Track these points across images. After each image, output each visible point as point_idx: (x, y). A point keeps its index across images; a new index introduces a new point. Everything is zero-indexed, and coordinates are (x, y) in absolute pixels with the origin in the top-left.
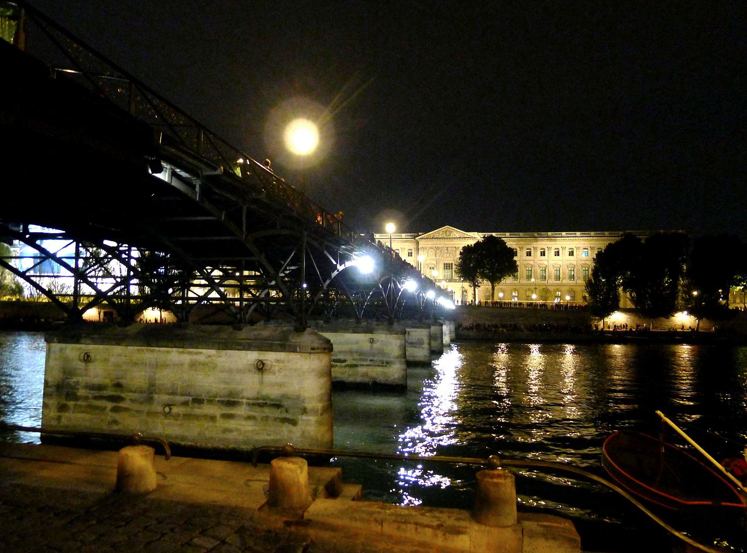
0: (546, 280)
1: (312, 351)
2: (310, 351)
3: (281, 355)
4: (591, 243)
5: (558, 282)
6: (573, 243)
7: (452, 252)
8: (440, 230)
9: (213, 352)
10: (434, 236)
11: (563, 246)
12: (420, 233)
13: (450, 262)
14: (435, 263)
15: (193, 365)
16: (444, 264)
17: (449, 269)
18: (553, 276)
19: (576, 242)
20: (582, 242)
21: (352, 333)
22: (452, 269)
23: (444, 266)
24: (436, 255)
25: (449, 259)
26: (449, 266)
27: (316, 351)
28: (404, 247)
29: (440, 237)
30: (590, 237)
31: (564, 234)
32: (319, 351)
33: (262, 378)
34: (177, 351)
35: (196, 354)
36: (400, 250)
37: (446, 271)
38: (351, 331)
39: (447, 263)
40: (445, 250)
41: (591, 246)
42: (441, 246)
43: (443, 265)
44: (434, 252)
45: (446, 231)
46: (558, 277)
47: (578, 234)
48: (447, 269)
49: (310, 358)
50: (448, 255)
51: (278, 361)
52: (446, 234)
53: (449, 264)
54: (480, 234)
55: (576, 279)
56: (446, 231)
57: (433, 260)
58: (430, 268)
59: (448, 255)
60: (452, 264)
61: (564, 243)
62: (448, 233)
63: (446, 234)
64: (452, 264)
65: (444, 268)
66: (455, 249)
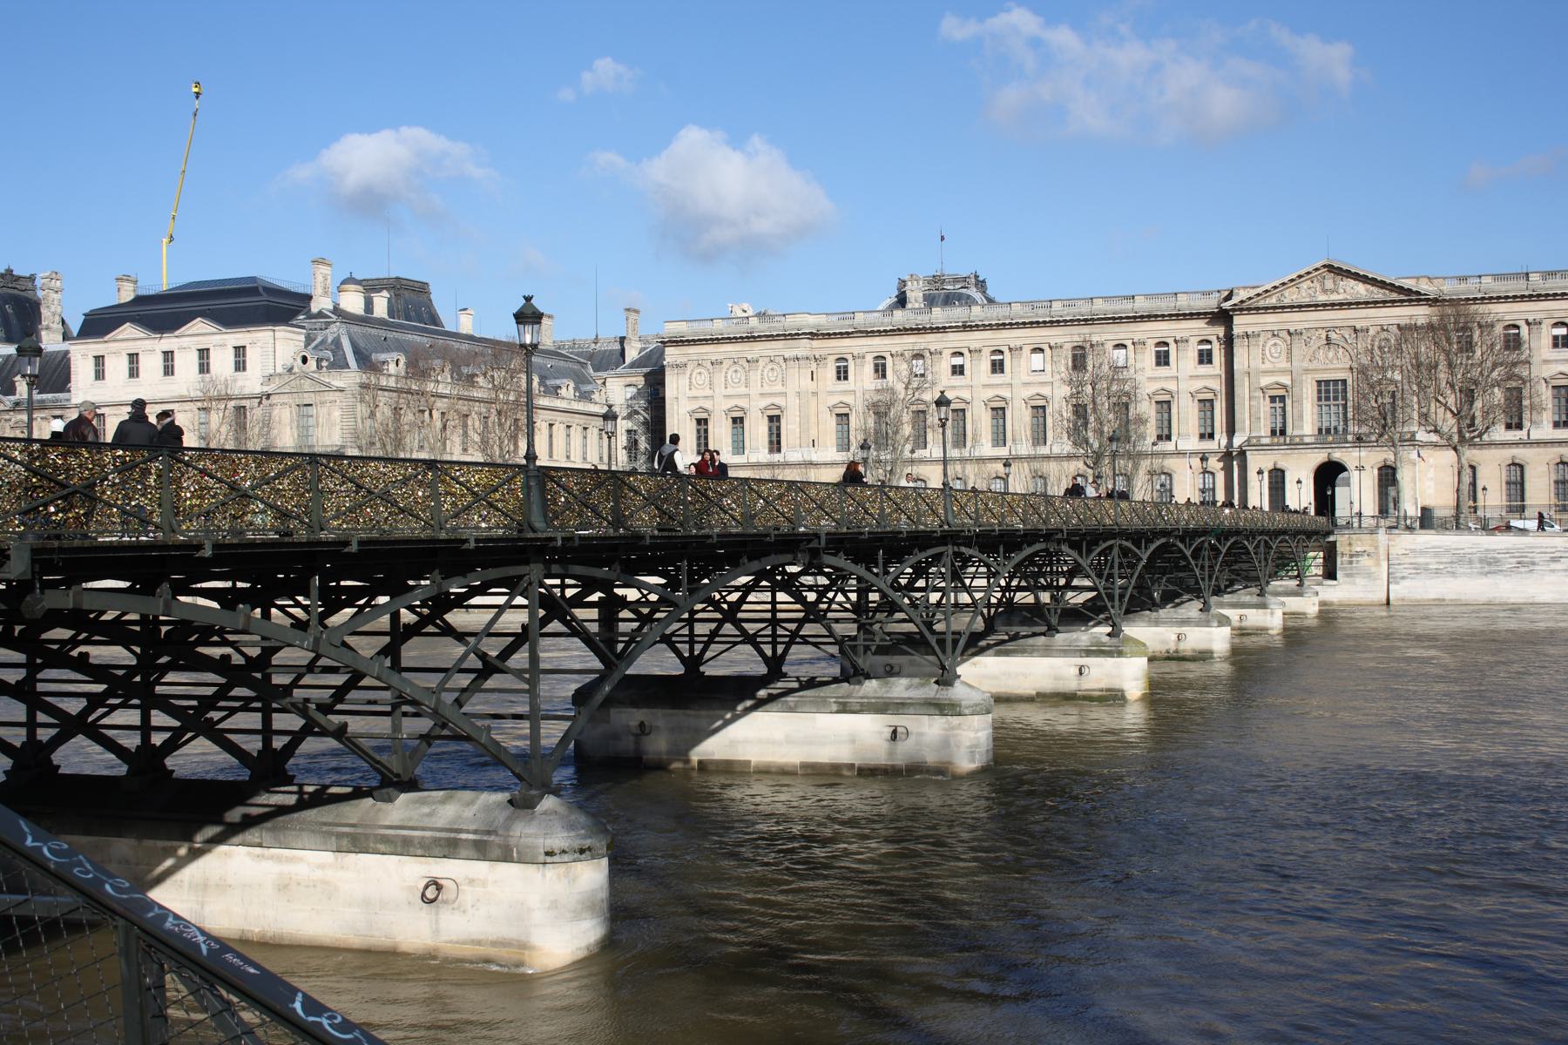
1: (549, 859)
2: (542, 858)
3: (480, 868)
9: (327, 857)
15: (283, 887)
21: (838, 712)
22: (1345, 398)
23: (1319, 392)
24: (1290, 358)
27: (556, 859)
32: (566, 858)
33: (437, 921)
34: (249, 854)
35: (290, 860)
38: (835, 707)
44: (1284, 346)
48: (1328, 399)
49: (544, 875)
50: (1331, 354)
51: (471, 882)
57: (1282, 372)
58: (1273, 399)
59: (1331, 354)
60: (1344, 381)
65: (1319, 399)
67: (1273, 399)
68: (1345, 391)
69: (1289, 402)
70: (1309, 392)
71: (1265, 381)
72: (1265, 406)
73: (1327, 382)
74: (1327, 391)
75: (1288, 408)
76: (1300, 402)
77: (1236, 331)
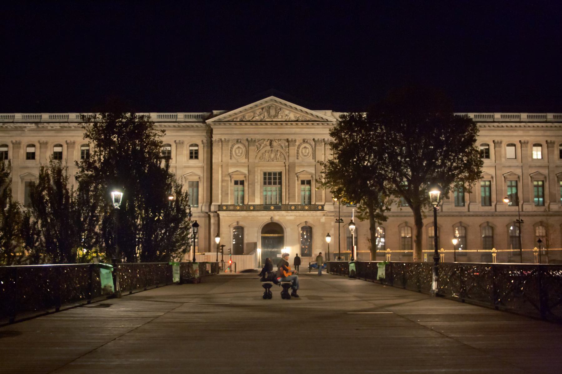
0: (466, 204)
4: (548, 133)
5: (487, 208)
6: (515, 134)
7: (280, 149)
8: (256, 106)
10: (244, 117)
11: (497, 139)
12: (215, 112)
13: (277, 170)
14: (246, 172)
16: (265, 174)
17: (275, 183)
18: (479, 199)
19: (520, 133)
20: (531, 133)
22: (280, 183)
23: (265, 179)
25: (275, 163)
26: (275, 179)
28: (181, 139)
29: (257, 118)
30: (494, 122)
31: (498, 116)
36: (38, 145)
37: (269, 188)
39: (269, 171)
40: (266, 145)
41: (549, 139)
42: (258, 137)
43: (263, 176)
44: (244, 149)
45: (269, 108)
46: (487, 199)
47: (524, 116)
48: (270, 183)
50: (272, 156)
52: (269, 112)
53: (275, 174)
54: (338, 114)
55: (521, 203)
56: (269, 108)
57: (242, 165)
58: (236, 183)
60: (280, 174)
61: (499, 133)
62: (273, 112)
63: (269, 112)
64: (280, 174)
65: (265, 183)
66: (287, 144)
67: (236, 183)
68: (280, 179)
69: (246, 184)
70: (259, 178)
71: (231, 170)
72: (231, 186)
73: (270, 174)
74: (270, 179)
75: (246, 188)
76: (252, 184)
77: (215, 138)
